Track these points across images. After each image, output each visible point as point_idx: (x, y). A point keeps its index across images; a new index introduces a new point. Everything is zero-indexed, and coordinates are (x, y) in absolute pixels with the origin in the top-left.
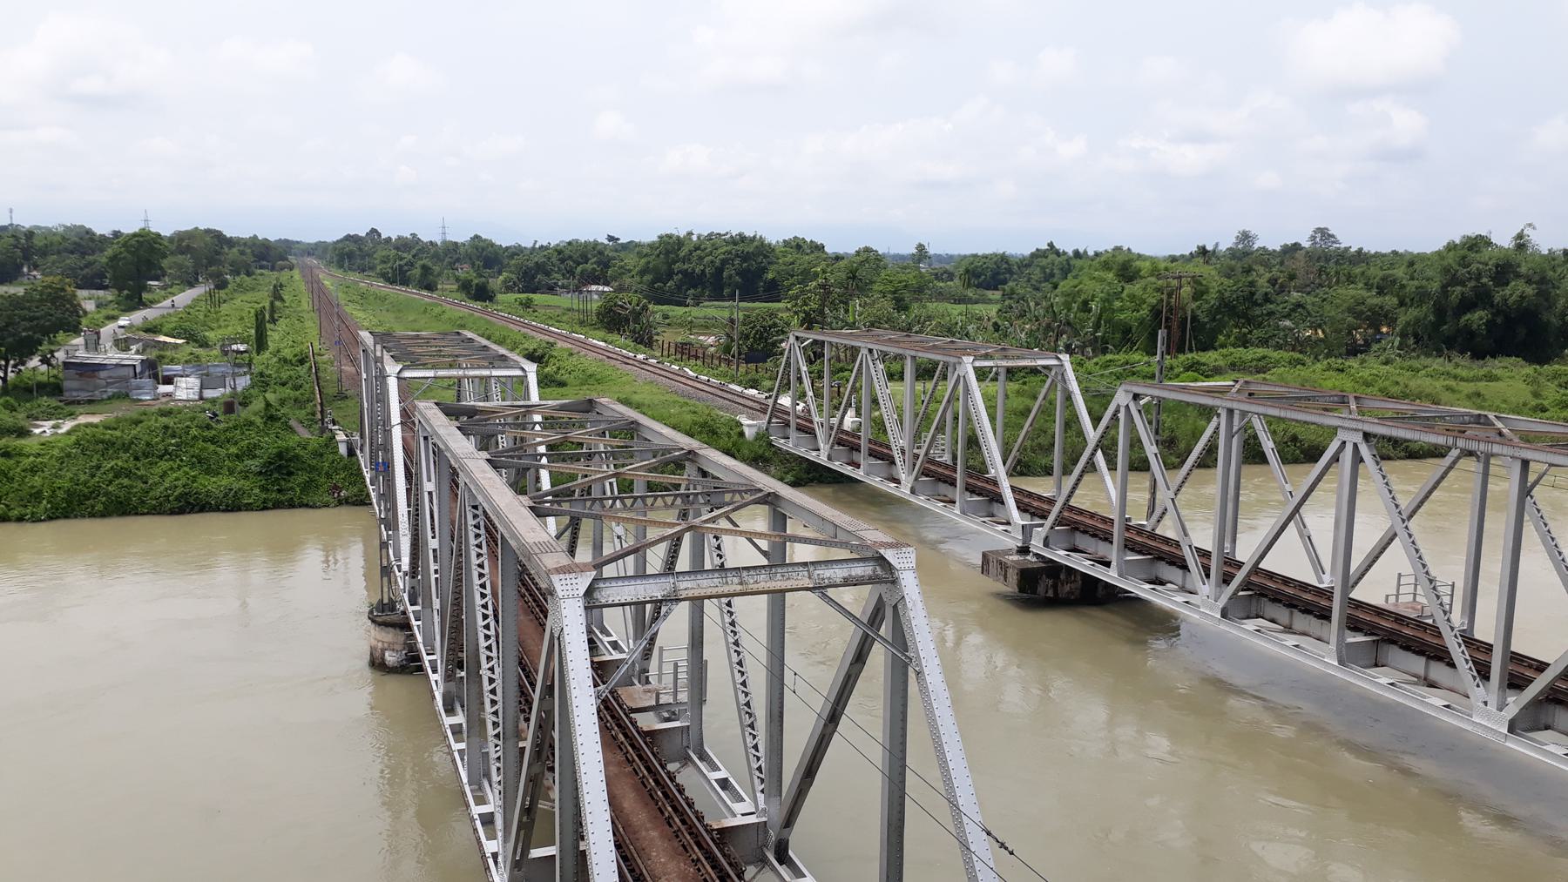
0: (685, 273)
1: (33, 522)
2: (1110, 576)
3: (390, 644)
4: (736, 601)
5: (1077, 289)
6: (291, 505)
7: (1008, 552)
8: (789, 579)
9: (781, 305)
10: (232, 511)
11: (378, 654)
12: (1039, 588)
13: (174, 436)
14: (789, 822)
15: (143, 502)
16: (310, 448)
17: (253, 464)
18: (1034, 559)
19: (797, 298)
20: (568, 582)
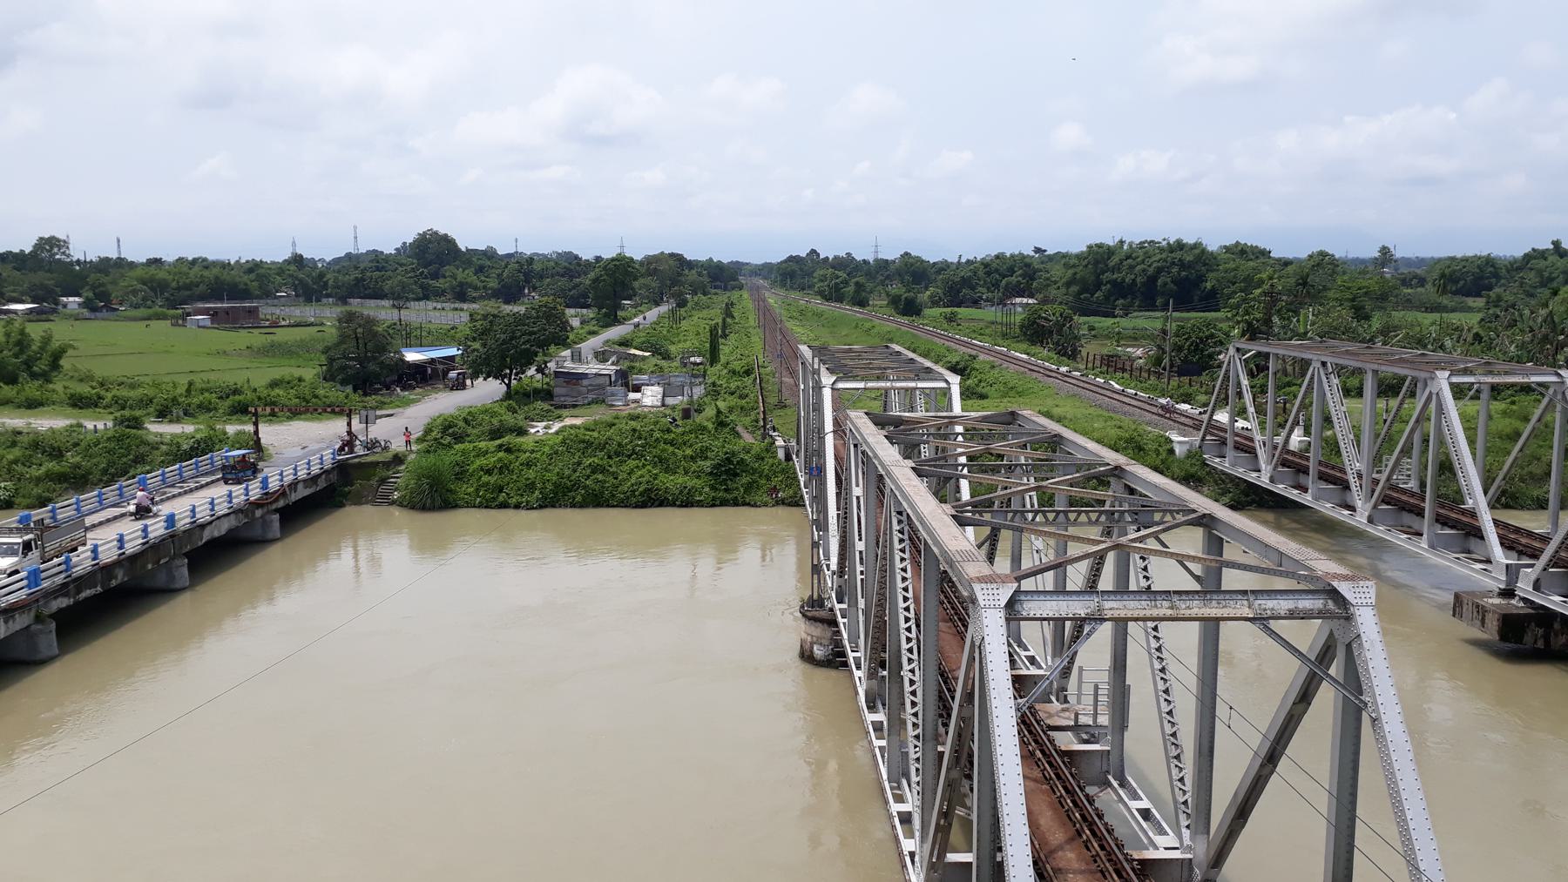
0: (1114, 283)
1: (528, 509)
3: (818, 637)
4: (1162, 626)
6: (736, 503)
7: (1489, 594)
10: (686, 506)
11: (807, 647)
13: (640, 438)
15: (614, 496)
16: (753, 452)
18: (1522, 604)
19: (1238, 306)
20: (990, 592)
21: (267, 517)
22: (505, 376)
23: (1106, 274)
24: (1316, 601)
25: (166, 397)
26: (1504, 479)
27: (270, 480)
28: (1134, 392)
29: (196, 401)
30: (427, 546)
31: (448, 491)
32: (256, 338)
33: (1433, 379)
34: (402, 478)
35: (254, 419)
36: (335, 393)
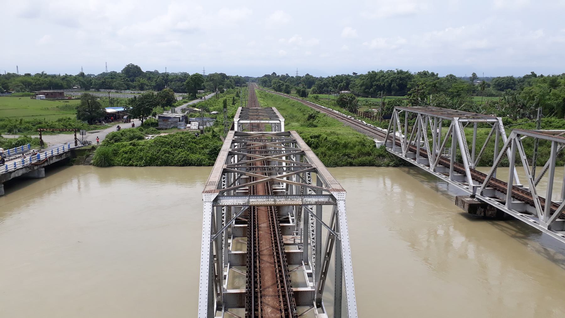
0: (377, 85)
2: (505, 209)
5: (531, 91)
8: (293, 200)
9: (405, 97)
12: (477, 212)
14: (320, 292)
15: (172, 162)
17: (207, 151)
19: (411, 94)
20: (208, 196)
21: (39, 169)
22: (141, 117)
23: (375, 82)
24: (326, 199)
25: (12, 125)
26: (480, 156)
27: (41, 156)
28: (370, 125)
29: (23, 127)
30: (105, 180)
31: (111, 160)
32: (61, 103)
33: (453, 120)
34: (94, 155)
35: (40, 133)
36: (79, 124)
